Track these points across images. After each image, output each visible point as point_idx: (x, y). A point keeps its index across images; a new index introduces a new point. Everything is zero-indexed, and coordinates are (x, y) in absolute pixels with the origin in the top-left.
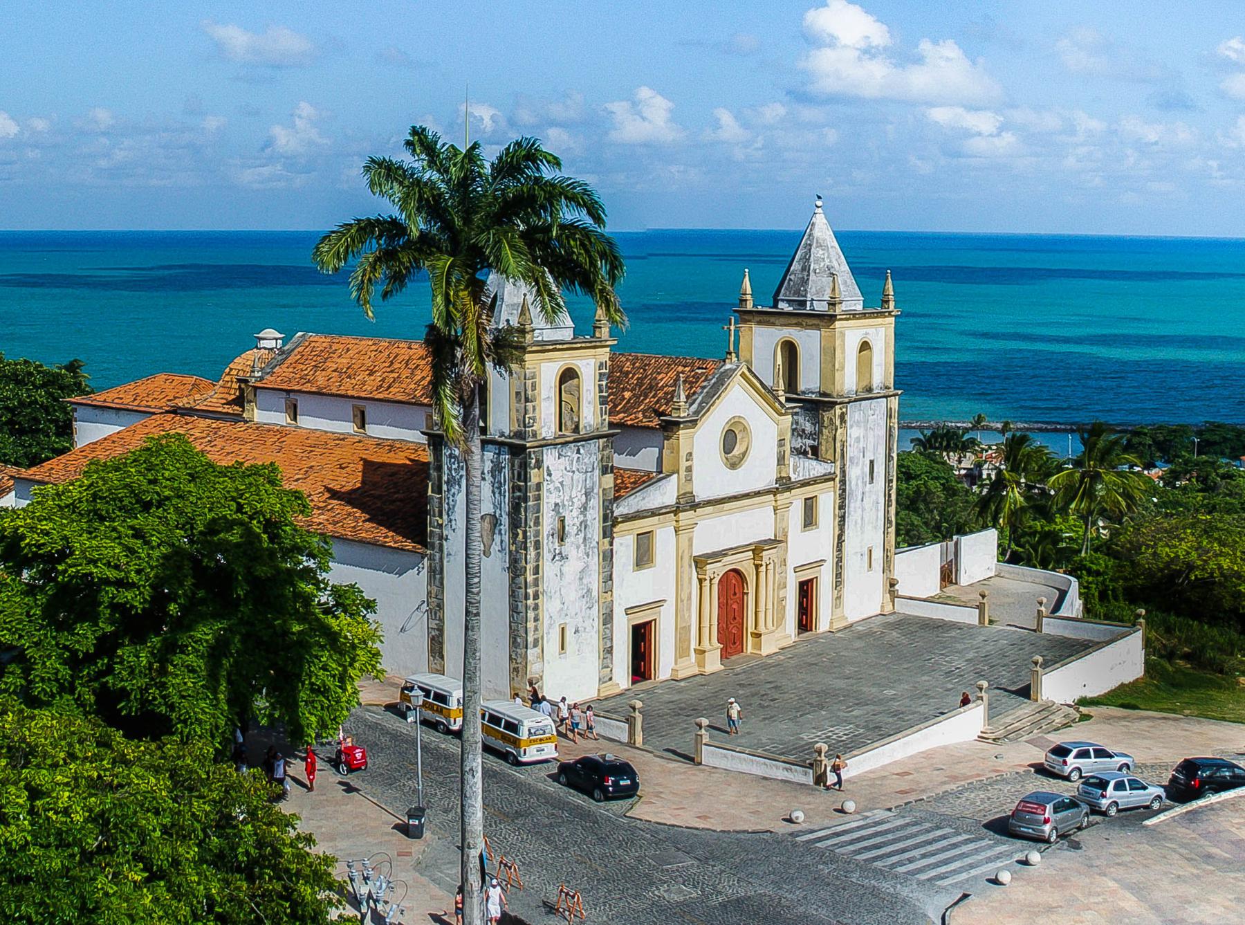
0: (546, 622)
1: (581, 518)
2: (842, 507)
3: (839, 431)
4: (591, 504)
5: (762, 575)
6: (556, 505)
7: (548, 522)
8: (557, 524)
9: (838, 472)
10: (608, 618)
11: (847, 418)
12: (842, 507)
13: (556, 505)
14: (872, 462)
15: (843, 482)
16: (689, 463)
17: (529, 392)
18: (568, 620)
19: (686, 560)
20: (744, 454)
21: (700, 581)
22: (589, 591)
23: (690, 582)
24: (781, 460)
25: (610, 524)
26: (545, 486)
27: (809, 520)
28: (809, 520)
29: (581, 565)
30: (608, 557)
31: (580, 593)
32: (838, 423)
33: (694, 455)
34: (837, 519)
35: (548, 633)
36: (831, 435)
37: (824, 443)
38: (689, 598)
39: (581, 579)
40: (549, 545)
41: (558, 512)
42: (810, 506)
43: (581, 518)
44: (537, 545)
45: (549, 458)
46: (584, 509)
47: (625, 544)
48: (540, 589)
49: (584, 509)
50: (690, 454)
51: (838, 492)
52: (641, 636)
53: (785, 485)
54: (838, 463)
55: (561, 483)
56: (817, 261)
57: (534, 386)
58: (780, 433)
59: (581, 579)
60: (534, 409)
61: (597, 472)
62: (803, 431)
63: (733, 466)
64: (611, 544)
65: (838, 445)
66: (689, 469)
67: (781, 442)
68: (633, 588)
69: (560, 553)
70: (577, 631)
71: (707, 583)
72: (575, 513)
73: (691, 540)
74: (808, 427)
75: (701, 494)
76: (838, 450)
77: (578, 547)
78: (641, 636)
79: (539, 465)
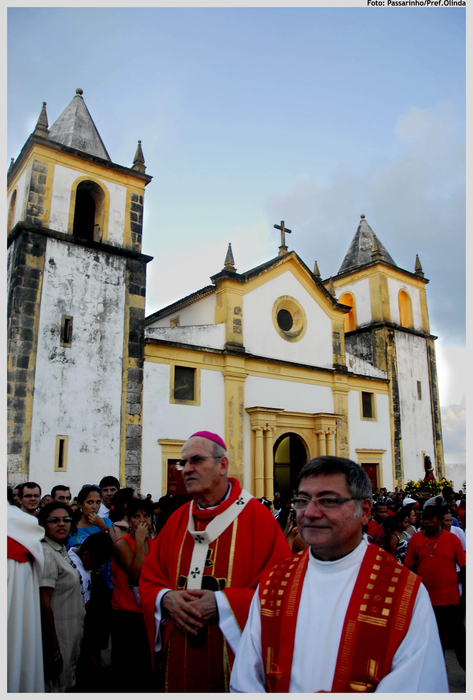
0: (36, 427)
1: (97, 326)
2: (396, 409)
3: (389, 348)
4: (113, 315)
5: (323, 443)
6: (60, 301)
7: (47, 316)
8: (60, 323)
9: (391, 378)
10: (133, 442)
11: (396, 339)
12: (396, 409)
13: (60, 301)
14: (419, 383)
15: (396, 389)
16: (237, 317)
17: (37, 182)
18: (69, 432)
19: (236, 407)
20: (299, 333)
21: (254, 431)
22: (106, 407)
23: (241, 431)
24: (337, 349)
27: (368, 410)
28: (368, 410)
29: (94, 377)
30: (136, 378)
31: (94, 406)
32: (388, 340)
33: (245, 311)
34: (393, 419)
35: (38, 441)
36: (383, 351)
37: (377, 358)
38: (241, 446)
39: (96, 390)
40: (46, 342)
41: (63, 310)
42: (367, 398)
43: (97, 326)
45: (53, 249)
46: (101, 318)
47: (158, 374)
48: (29, 385)
49: (101, 318)
50: (240, 310)
51: (392, 397)
53: (340, 370)
54: (390, 373)
55: (70, 282)
56: (364, 244)
57: (43, 180)
58: (335, 327)
59: (96, 390)
60: (41, 200)
61: (123, 288)
62: (362, 355)
64: (141, 365)
65: (389, 358)
66: (238, 322)
67: (336, 334)
69: (63, 354)
70: (84, 449)
71: (260, 434)
72: (89, 318)
73: (241, 391)
74: (365, 351)
75: (251, 347)
76: (390, 362)
77: (90, 356)
79: (39, 251)
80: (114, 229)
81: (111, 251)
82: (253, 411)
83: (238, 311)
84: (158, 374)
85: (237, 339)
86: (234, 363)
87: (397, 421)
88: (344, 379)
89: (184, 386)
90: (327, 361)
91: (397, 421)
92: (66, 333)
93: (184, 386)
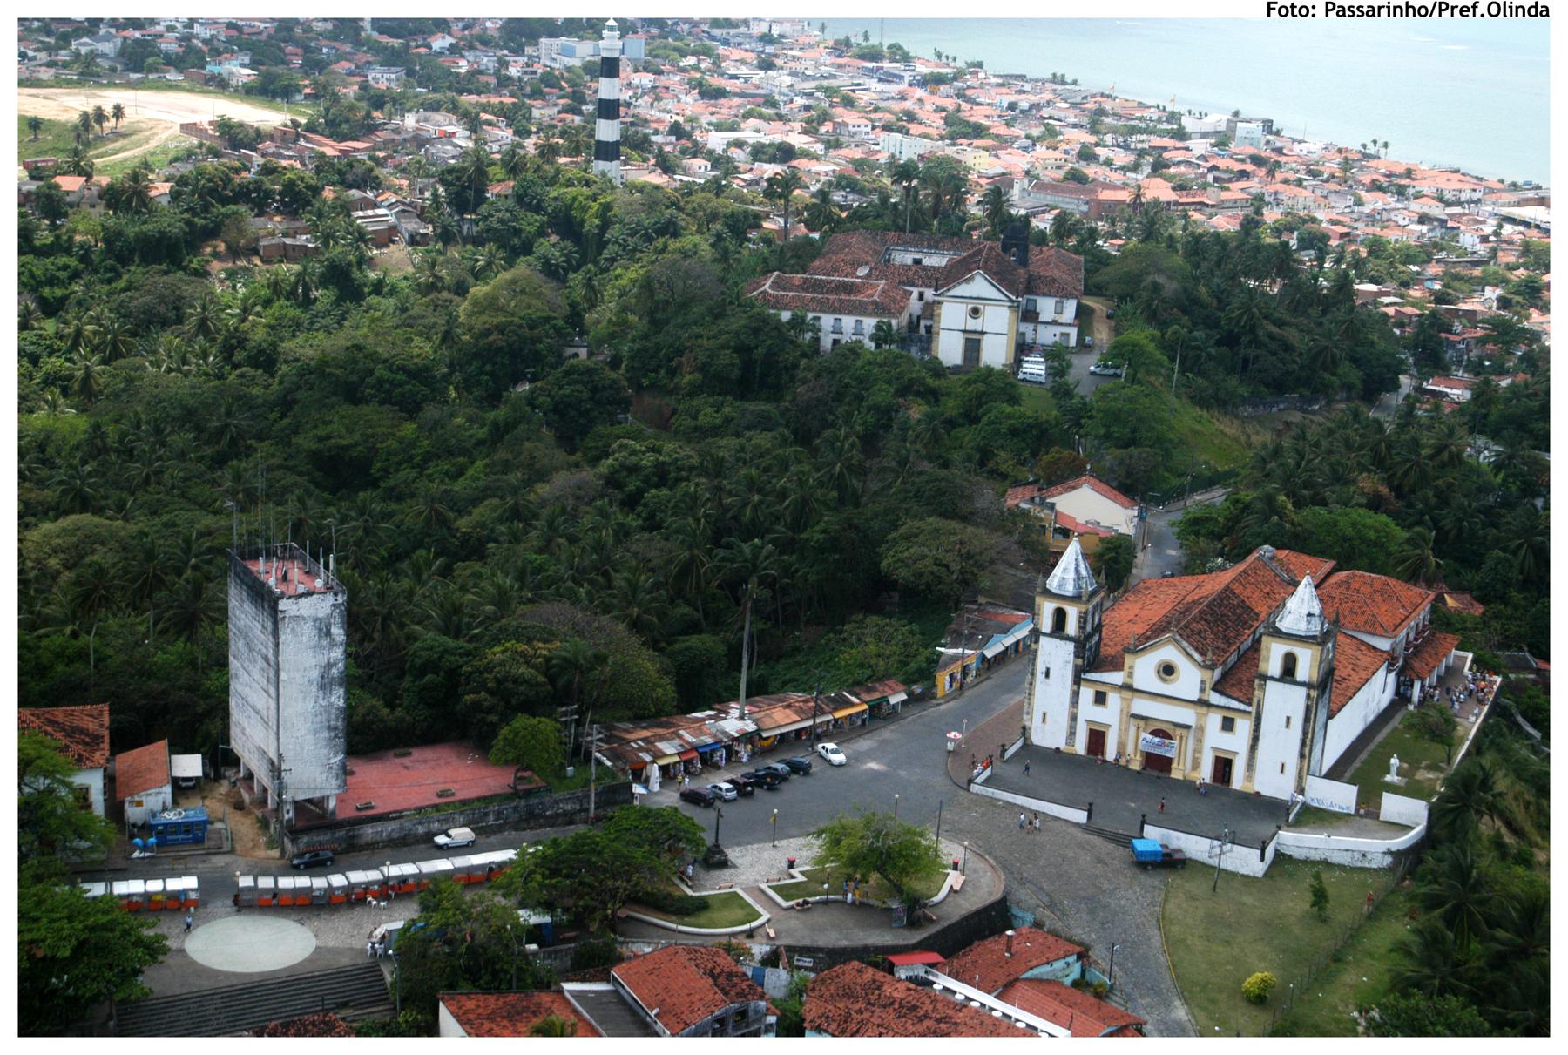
7: (1040, 668)
10: (1074, 718)
24: (1202, 690)
25: (1077, 680)
26: (1040, 653)
28: (1228, 725)
30: (1076, 695)
40: (1040, 676)
44: (1033, 674)
45: (1042, 639)
47: (1087, 694)
52: (1097, 738)
53: (1202, 703)
63: (1164, 680)
67: (1203, 682)
68: (1088, 710)
78: (1097, 738)
79: (1037, 641)
80: (1072, 627)
81: (1069, 638)
82: (1133, 716)
83: (1131, 667)
84: (1087, 694)
85: (1129, 681)
86: (1128, 694)
87: (1255, 739)
88: (1204, 710)
89: (1100, 699)
90: (1195, 696)
91: (1255, 739)
92: (1047, 675)
93: (1100, 699)
